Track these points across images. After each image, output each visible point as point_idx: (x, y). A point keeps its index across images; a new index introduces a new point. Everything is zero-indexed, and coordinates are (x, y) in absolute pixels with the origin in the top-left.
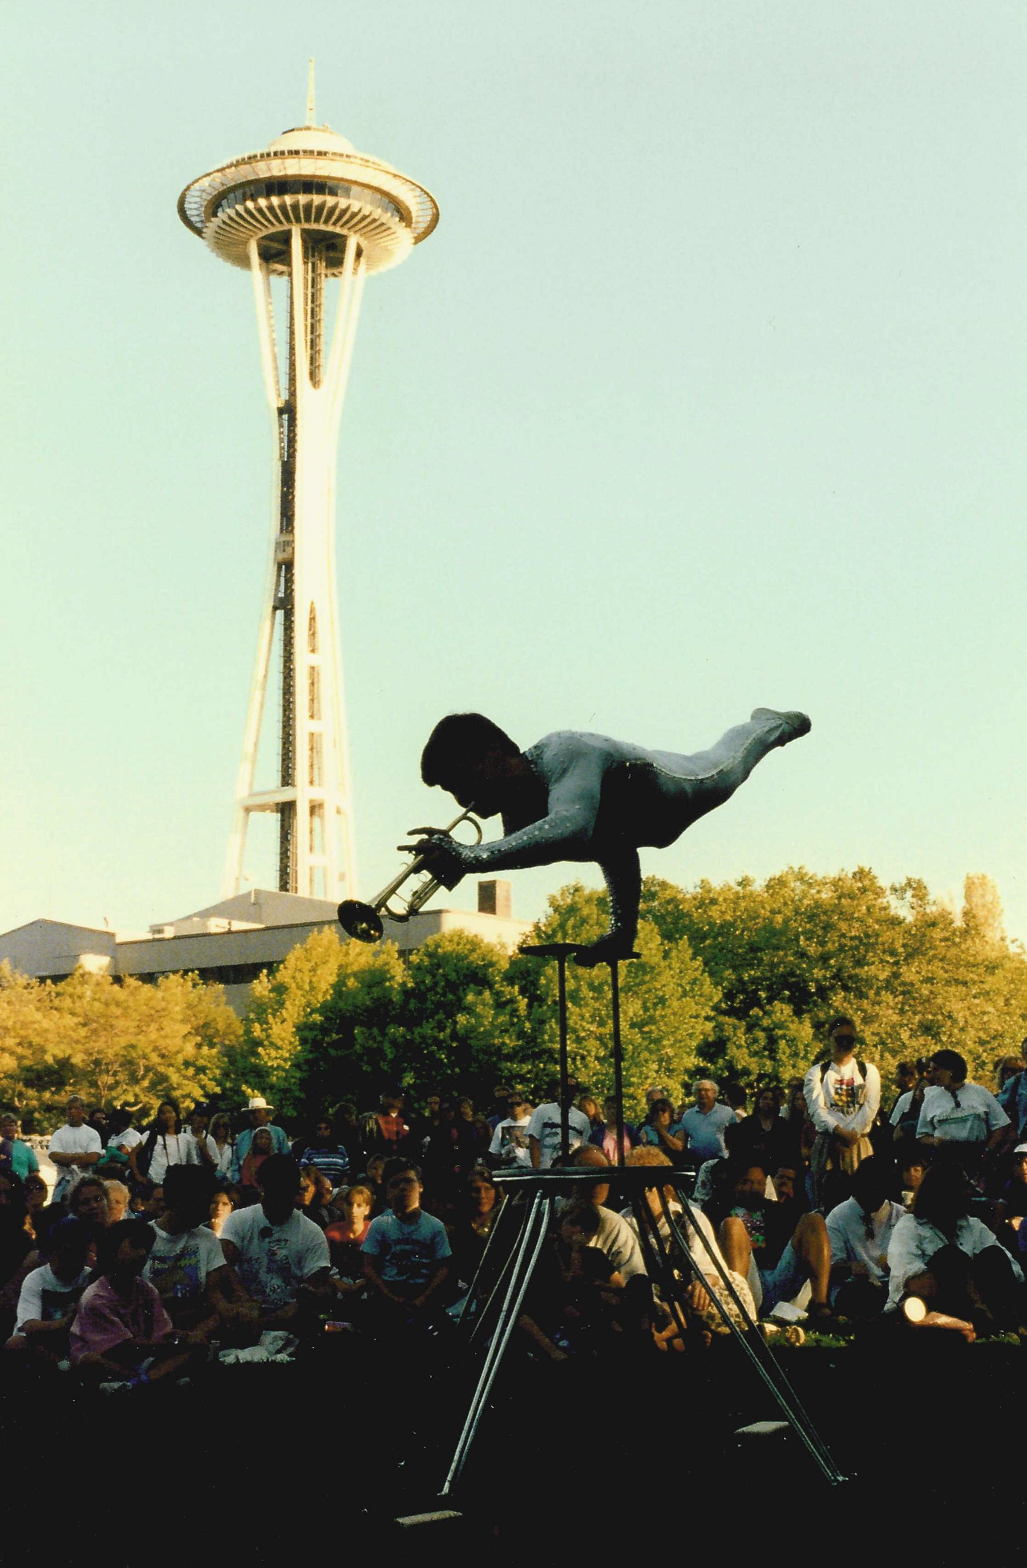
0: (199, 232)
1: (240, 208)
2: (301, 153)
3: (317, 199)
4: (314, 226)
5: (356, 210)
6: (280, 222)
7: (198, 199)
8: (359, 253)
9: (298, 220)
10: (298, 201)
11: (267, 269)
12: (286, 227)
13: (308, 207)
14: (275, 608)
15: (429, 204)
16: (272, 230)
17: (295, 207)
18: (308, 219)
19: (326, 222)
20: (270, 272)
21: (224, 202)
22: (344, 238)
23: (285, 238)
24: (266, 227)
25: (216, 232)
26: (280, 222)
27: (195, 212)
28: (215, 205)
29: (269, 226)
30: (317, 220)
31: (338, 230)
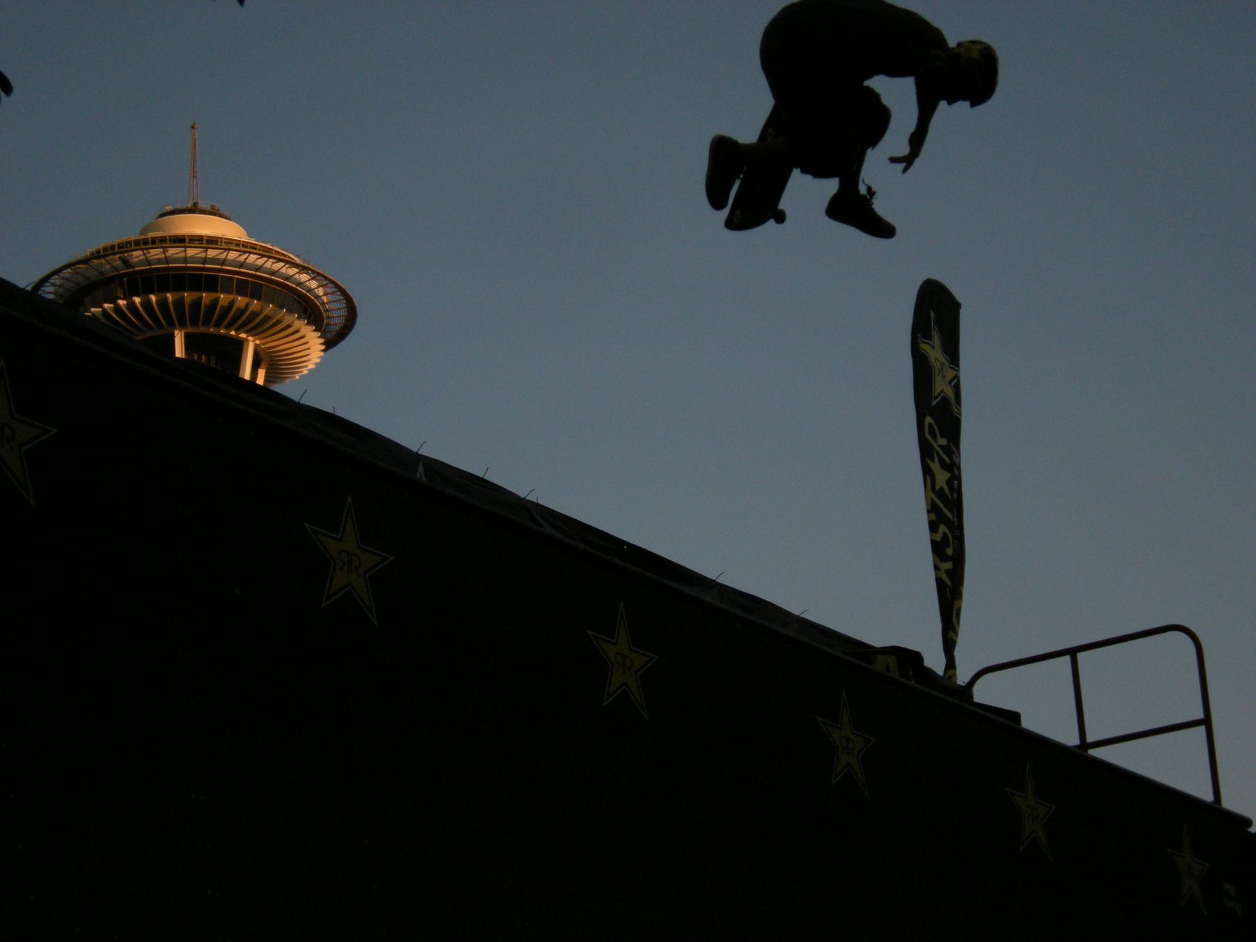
2: (187, 241)
3: (206, 296)
4: (202, 329)
5: (259, 310)
6: (159, 324)
9: (182, 325)
10: (183, 297)
13: (196, 304)
15: (343, 304)
16: (148, 334)
17: (179, 303)
18: (194, 322)
19: (218, 325)
21: (87, 300)
22: (240, 345)
24: (141, 330)
29: (145, 329)
30: (207, 322)
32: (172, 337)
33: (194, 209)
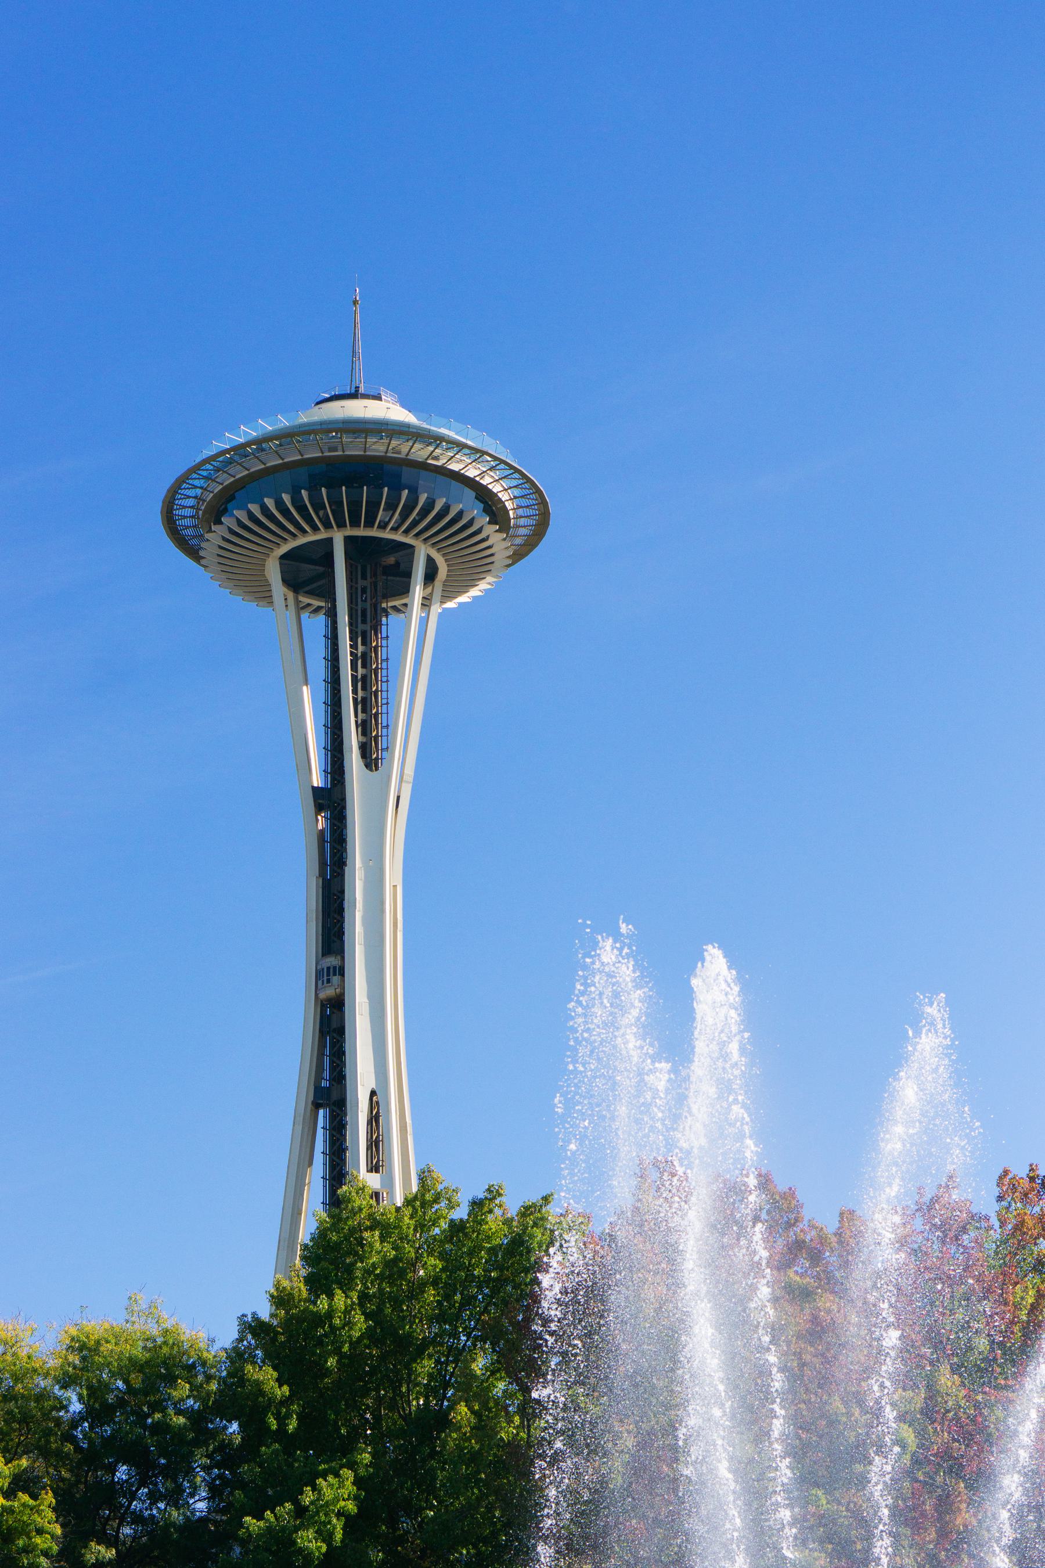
0: (194, 553)
1: (254, 508)
7: (191, 502)
8: (430, 576)
9: (341, 525)
11: (297, 602)
12: (322, 535)
14: (317, 1106)
16: (302, 540)
18: (355, 523)
20: (300, 608)
23: (324, 554)
25: (221, 547)
26: (315, 529)
27: (186, 522)
28: (216, 511)
30: (369, 524)
31: (399, 537)
32: (330, 541)
33: (354, 395)
